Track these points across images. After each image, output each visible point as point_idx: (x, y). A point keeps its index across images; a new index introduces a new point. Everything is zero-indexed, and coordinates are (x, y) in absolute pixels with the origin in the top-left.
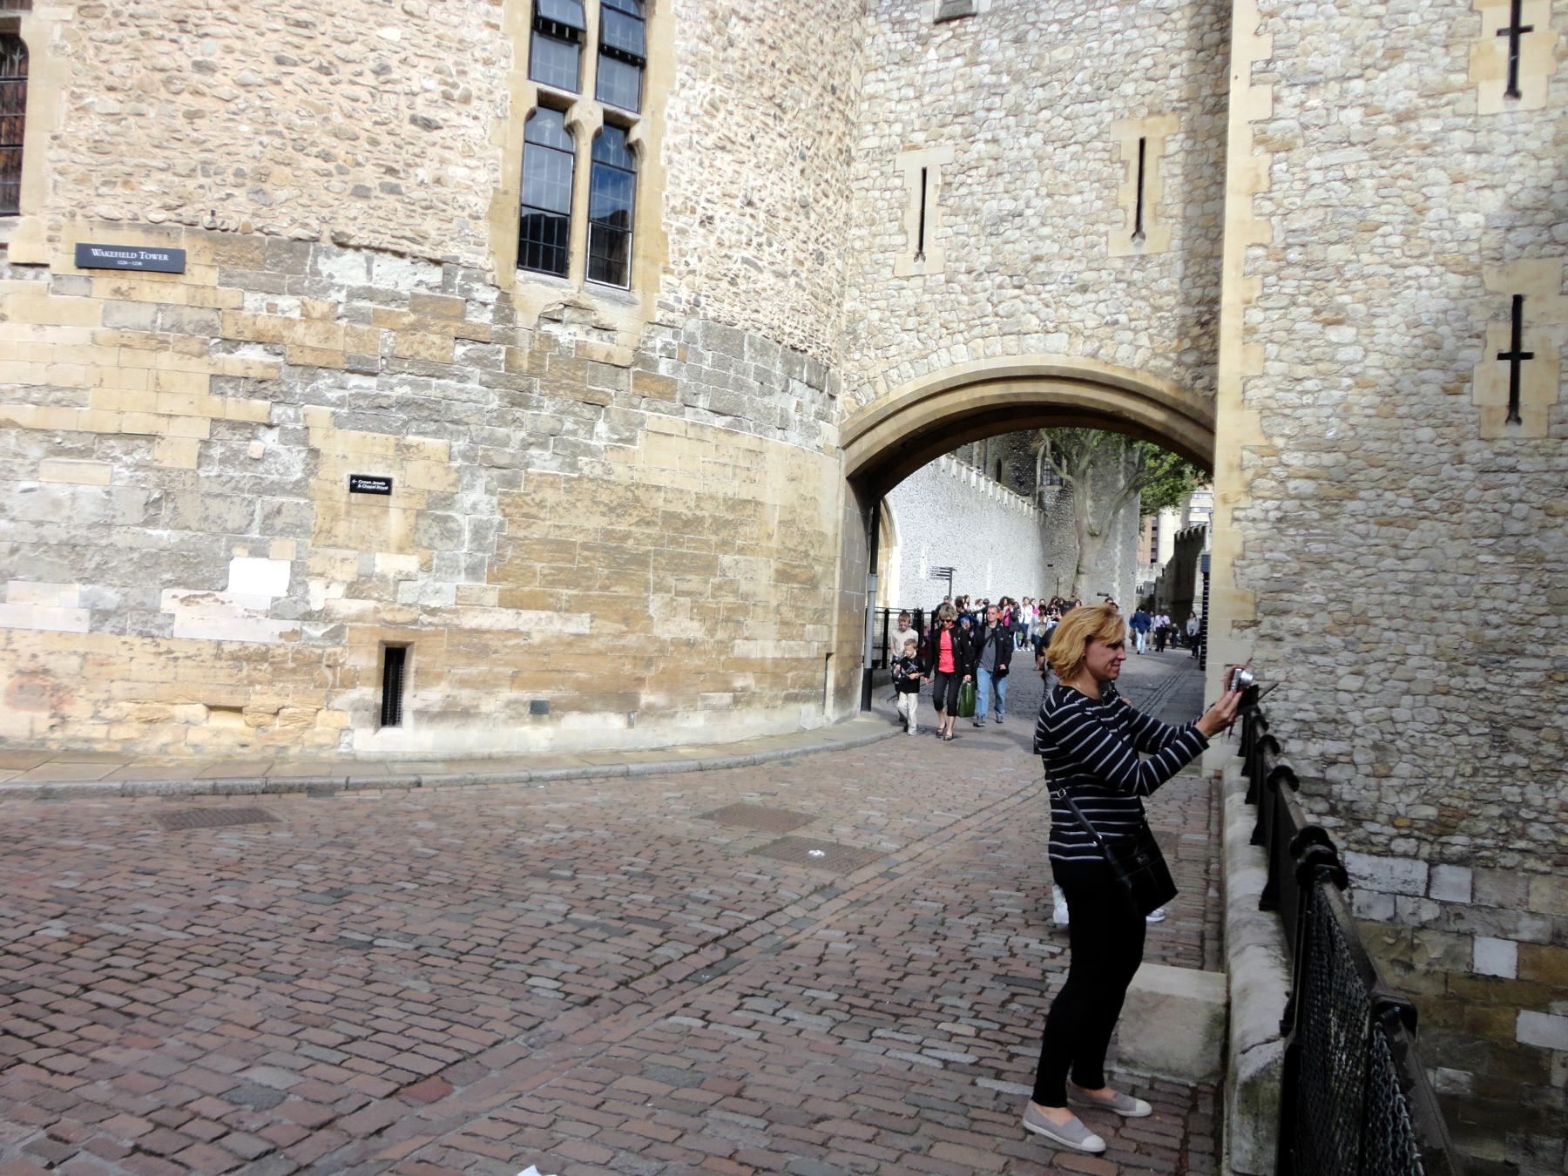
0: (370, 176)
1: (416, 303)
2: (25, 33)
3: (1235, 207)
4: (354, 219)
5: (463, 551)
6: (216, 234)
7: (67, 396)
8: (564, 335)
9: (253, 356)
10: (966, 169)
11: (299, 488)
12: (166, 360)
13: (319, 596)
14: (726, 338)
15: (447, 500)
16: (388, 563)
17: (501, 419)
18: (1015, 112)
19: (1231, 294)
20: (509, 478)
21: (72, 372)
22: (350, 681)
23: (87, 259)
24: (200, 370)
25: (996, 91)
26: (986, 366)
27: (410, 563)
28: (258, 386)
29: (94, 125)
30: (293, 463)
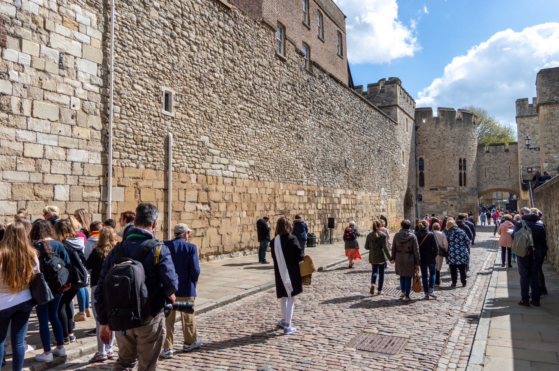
0: (450, 181)
2: (424, 172)
4: (449, 184)
6: (440, 187)
7: (430, 200)
8: (463, 191)
9: (443, 196)
10: (490, 168)
11: (447, 206)
12: (437, 197)
14: (472, 188)
15: (456, 206)
21: (430, 198)
23: (430, 189)
24: (440, 197)
26: (494, 188)
27: (455, 211)
29: (430, 179)
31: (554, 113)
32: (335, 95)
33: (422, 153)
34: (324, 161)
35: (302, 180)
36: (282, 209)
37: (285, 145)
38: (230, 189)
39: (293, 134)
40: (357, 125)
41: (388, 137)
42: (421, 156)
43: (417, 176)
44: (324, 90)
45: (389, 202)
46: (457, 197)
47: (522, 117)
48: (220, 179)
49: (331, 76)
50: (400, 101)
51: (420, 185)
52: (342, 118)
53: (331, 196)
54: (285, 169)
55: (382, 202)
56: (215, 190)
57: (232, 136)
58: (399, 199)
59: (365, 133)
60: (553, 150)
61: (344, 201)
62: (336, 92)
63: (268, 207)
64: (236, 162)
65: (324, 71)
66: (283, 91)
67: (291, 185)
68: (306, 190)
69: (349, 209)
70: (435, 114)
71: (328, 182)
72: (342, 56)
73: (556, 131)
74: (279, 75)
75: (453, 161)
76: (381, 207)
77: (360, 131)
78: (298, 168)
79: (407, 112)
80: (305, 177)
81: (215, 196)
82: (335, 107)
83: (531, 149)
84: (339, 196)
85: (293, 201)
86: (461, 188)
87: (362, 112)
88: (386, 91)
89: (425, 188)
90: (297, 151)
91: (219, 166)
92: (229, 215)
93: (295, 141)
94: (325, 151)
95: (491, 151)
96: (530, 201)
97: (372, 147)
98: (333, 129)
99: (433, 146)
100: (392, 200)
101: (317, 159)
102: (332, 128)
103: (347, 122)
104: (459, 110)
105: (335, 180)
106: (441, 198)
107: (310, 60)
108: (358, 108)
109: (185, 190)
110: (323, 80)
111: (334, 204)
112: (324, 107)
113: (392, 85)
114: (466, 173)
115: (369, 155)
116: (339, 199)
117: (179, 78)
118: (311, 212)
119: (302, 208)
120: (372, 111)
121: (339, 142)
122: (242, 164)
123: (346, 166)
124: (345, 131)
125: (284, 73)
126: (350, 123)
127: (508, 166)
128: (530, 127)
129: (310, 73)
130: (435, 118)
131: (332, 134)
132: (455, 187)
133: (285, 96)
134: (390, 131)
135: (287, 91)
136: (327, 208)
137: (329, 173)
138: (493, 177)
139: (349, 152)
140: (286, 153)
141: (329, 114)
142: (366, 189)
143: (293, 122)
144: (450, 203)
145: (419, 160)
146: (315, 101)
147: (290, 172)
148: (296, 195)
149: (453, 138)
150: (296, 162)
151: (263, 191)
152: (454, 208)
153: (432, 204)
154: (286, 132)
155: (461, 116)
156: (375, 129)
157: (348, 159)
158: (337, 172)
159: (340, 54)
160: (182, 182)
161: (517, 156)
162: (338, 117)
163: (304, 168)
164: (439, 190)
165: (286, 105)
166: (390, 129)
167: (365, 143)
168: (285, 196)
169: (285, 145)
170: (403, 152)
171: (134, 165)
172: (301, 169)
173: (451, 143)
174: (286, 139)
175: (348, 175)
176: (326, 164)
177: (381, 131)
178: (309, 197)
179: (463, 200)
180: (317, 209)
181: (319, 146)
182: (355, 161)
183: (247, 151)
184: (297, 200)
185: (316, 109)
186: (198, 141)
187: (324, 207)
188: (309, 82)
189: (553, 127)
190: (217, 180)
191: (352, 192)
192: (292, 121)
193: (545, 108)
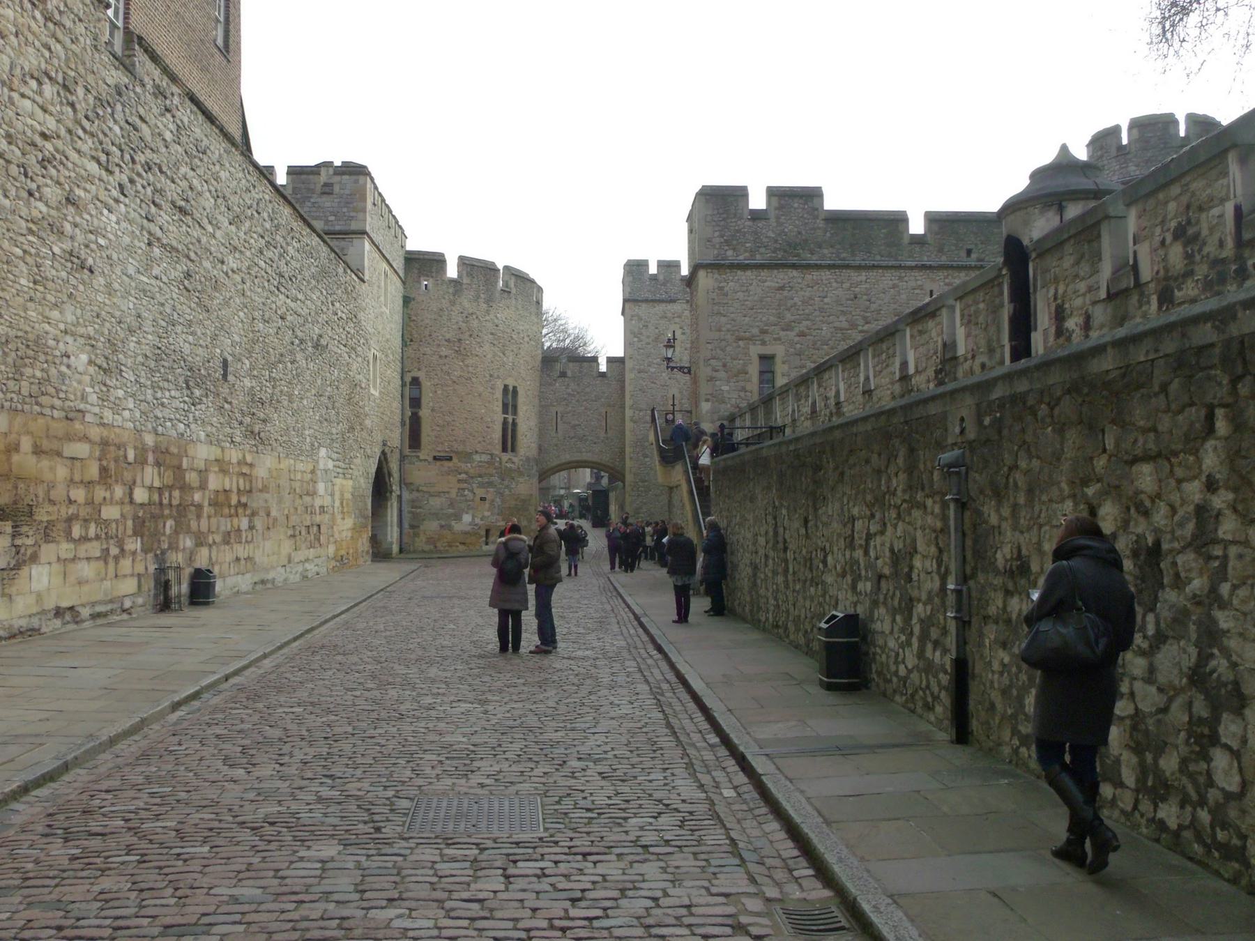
1: (487, 463)
3: (627, 433)
5: (496, 511)
6: (457, 453)
8: (509, 465)
9: (463, 476)
11: (473, 500)
13: (477, 521)
14: (528, 459)
15: (493, 501)
16: (487, 514)
17: (501, 483)
18: (578, 401)
19: (628, 450)
20: (502, 494)
22: (481, 537)
25: (573, 395)
26: (574, 459)
27: (489, 514)
28: (465, 481)
30: (470, 496)
31: (726, 289)
32: (201, 160)
33: (416, 364)
34: (160, 353)
35: (82, 406)
37: (23, 281)
39: (56, 250)
40: (262, 264)
41: (340, 313)
42: (415, 374)
43: (403, 424)
44: (168, 136)
45: (336, 488)
46: (496, 479)
47: (635, 301)
49: (193, 99)
50: (371, 223)
51: (410, 447)
52: (219, 234)
53: (175, 462)
54: (19, 362)
55: (321, 487)
58: (362, 481)
59: (283, 290)
60: (722, 374)
61: (214, 482)
62: (205, 153)
65: (173, 78)
66: (23, 96)
67: (41, 421)
68: (97, 439)
69: (230, 506)
70: (452, 271)
71: (170, 420)
72: (228, 52)
73: (728, 331)
74: (12, 38)
75: (489, 390)
76: (318, 502)
77: (269, 281)
78: (69, 366)
79: (388, 256)
80: (93, 398)
82: (200, 194)
83: (673, 368)
84: (202, 466)
85: (48, 476)
86: (505, 457)
87: (277, 227)
88: (336, 189)
89: (423, 454)
90: (69, 308)
93: (64, 274)
94: (164, 324)
95: (569, 374)
96: (684, 487)
97: (299, 334)
98: (192, 261)
99: (444, 351)
100: (345, 482)
101: (138, 343)
102: (188, 257)
103: (235, 248)
104: (506, 268)
105: (191, 416)
106: (459, 481)
107: (126, 28)
108: (265, 215)
110: (168, 102)
111: (185, 488)
112: (163, 182)
113: (354, 177)
114: (517, 421)
115: (292, 352)
116: (203, 473)
118: (110, 512)
119: (81, 499)
120: (304, 233)
121: (207, 302)
123: (225, 376)
124: (227, 274)
125: (31, 38)
126: (241, 252)
127: (603, 411)
128: (650, 325)
129: (124, 63)
130: (452, 281)
131: (188, 275)
132: (491, 455)
133: (32, 116)
134: (345, 297)
135: (38, 99)
136: (165, 501)
137: (173, 393)
138: (572, 434)
139: (237, 338)
140: (26, 309)
141: (182, 210)
142: (280, 449)
143: (58, 209)
144: (480, 492)
145: (411, 384)
146: (137, 158)
147: (38, 374)
148: (59, 454)
149: (492, 334)
150: (61, 344)
152: (487, 505)
153: (438, 494)
154: (31, 238)
155: (512, 284)
156: (309, 282)
157: (233, 355)
158: (197, 393)
159: (220, 42)
161: (623, 388)
162: (210, 228)
163: (91, 369)
164: (455, 460)
165: (34, 145)
166: (347, 293)
167: (282, 318)
168: (16, 458)
169: (23, 281)
170: (375, 358)
172: (81, 369)
173: (487, 347)
174: (28, 259)
175: (230, 403)
176: (166, 364)
177: (325, 292)
178: (105, 463)
179: (507, 487)
180: (132, 501)
181: (145, 303)
182: (252, 368)
184: (62, 472)
185: (139, 188)
187: (156, 497)
188: (120, 94)
189: (723, 319)
191: (240, 456)
192: (53, 204)
193: (710, 275)
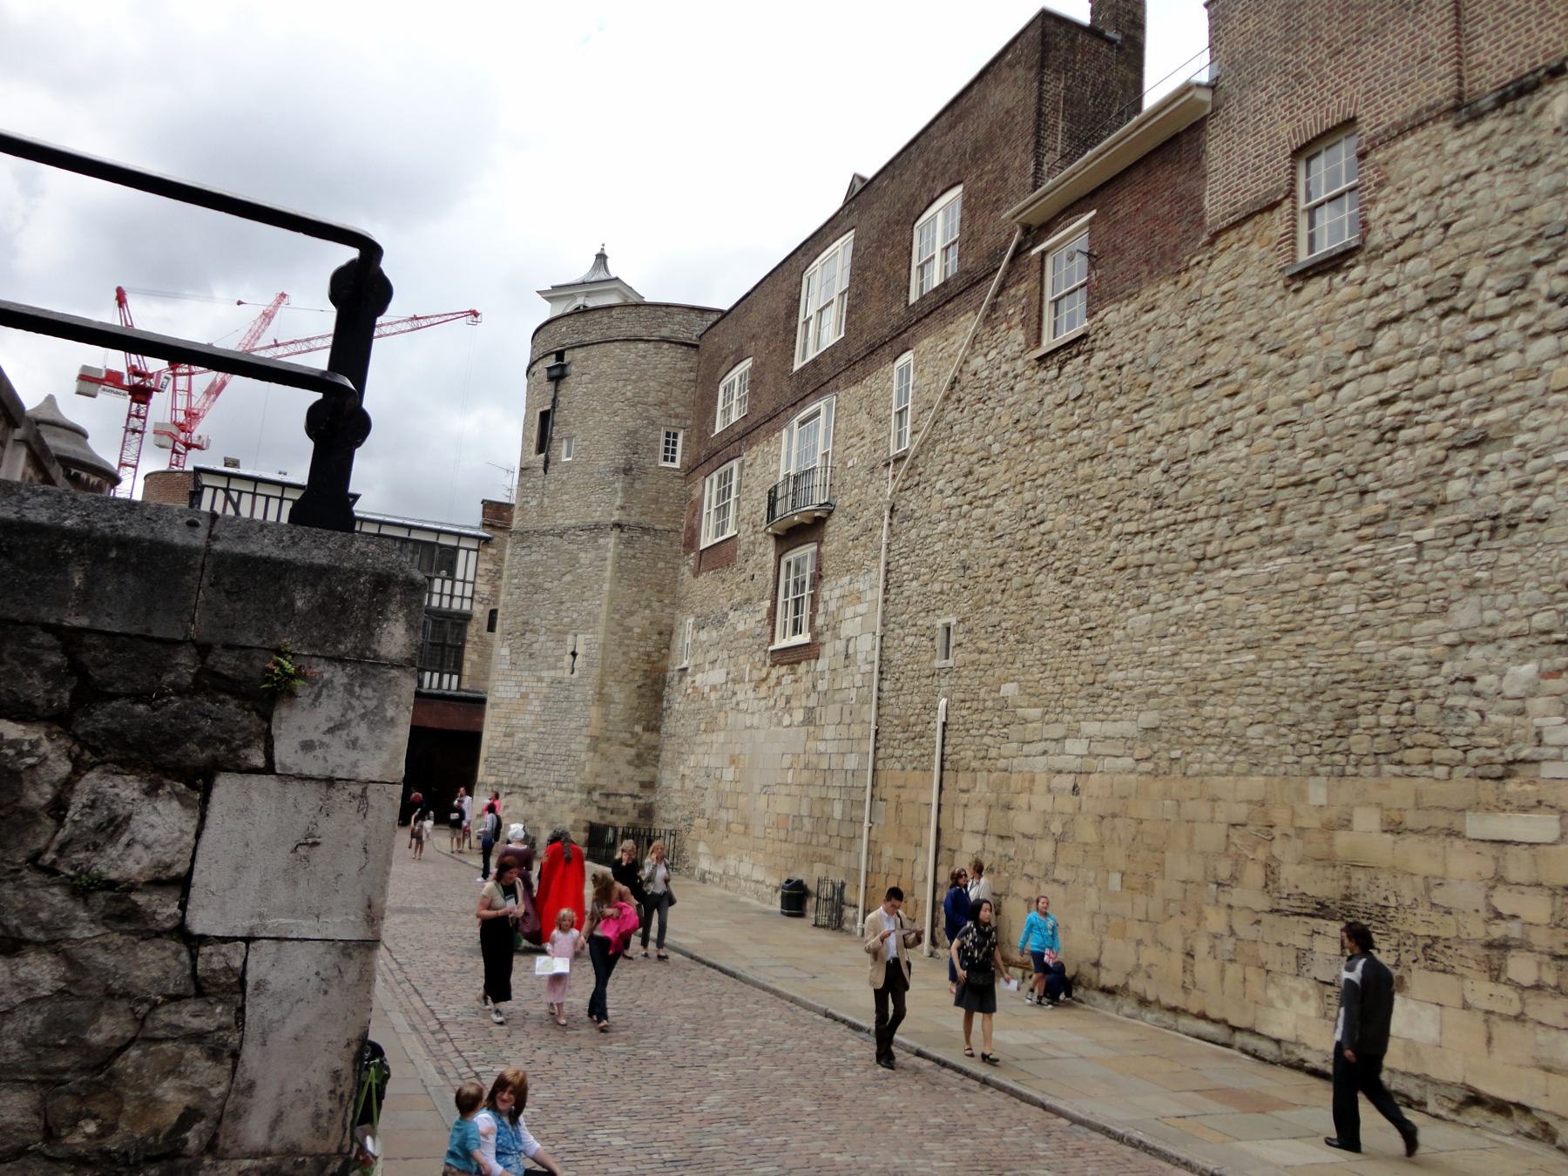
36: (1325, 887)
38: (1067, 803)
48: (1041, 779)
56: (1026, 807)
57: (1080, 659)
63: (1224, 871)
64: (1090, 727)
81: (1023, 822)
91: (1041, 746)
92: (1061, 873)
109: (966, 806)
117: (965, 587)
122: (1109, 728)
151: (1201, 810)
160: (963, 791)
168: (1342, 839)
171: (898, 766)
183: (1130, 688)
186: (994, 700)
190: (1033, 781)
